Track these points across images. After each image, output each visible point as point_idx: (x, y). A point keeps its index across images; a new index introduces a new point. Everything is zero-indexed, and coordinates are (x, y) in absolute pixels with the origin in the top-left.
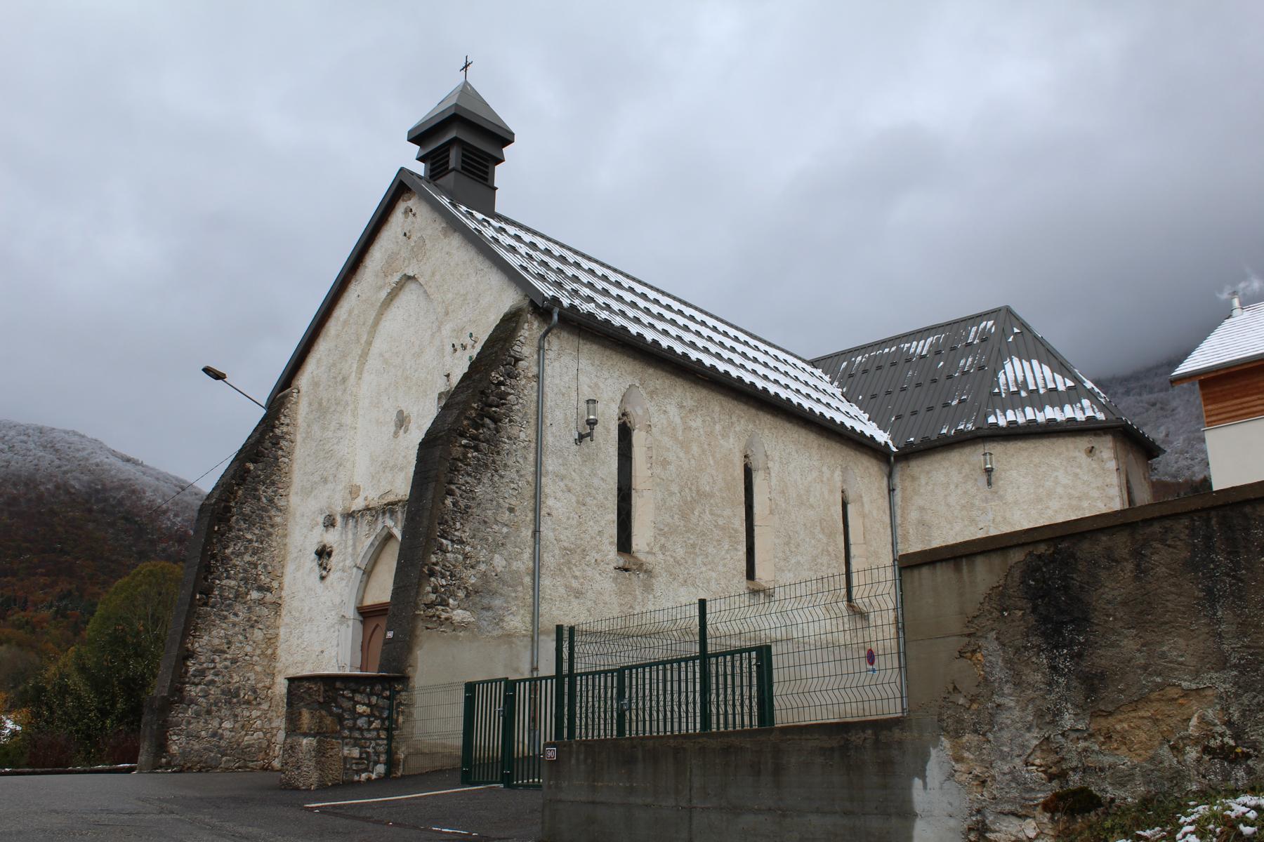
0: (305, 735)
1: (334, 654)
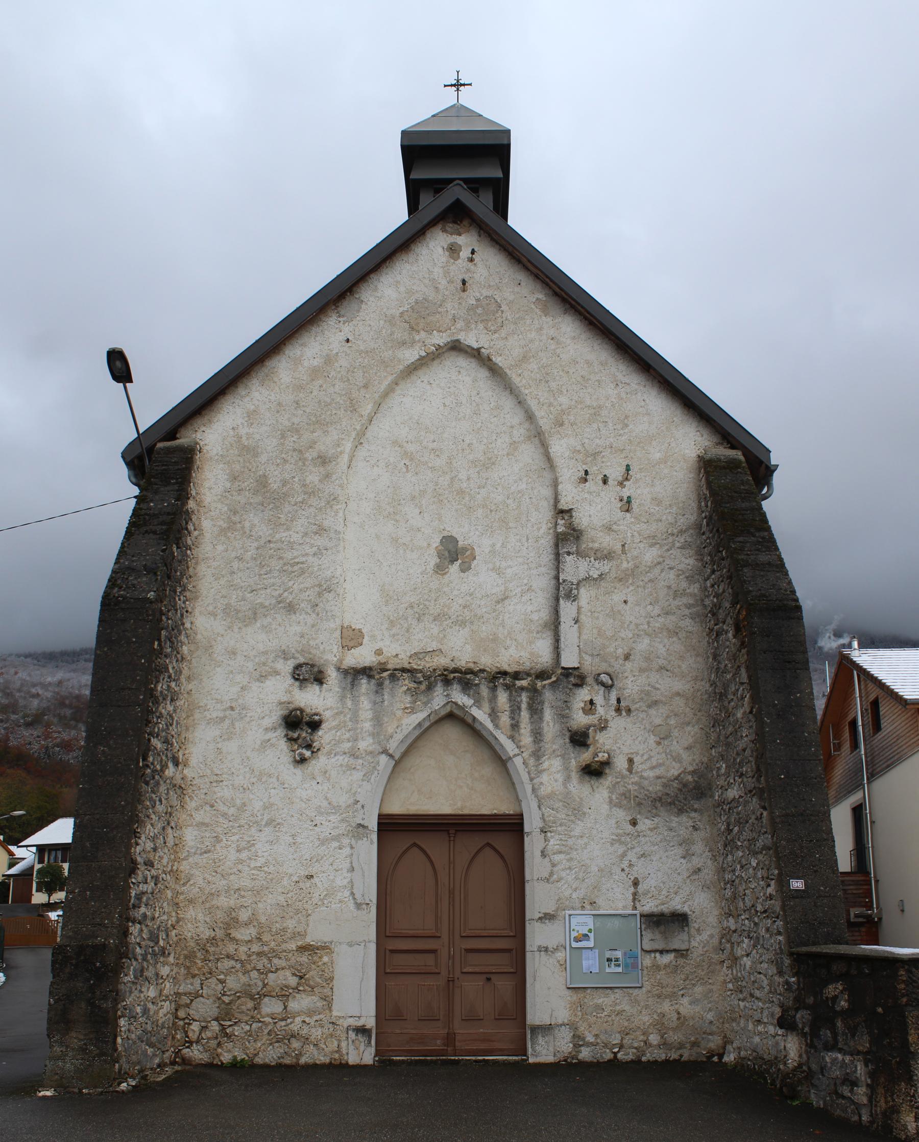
1: (341, 880)
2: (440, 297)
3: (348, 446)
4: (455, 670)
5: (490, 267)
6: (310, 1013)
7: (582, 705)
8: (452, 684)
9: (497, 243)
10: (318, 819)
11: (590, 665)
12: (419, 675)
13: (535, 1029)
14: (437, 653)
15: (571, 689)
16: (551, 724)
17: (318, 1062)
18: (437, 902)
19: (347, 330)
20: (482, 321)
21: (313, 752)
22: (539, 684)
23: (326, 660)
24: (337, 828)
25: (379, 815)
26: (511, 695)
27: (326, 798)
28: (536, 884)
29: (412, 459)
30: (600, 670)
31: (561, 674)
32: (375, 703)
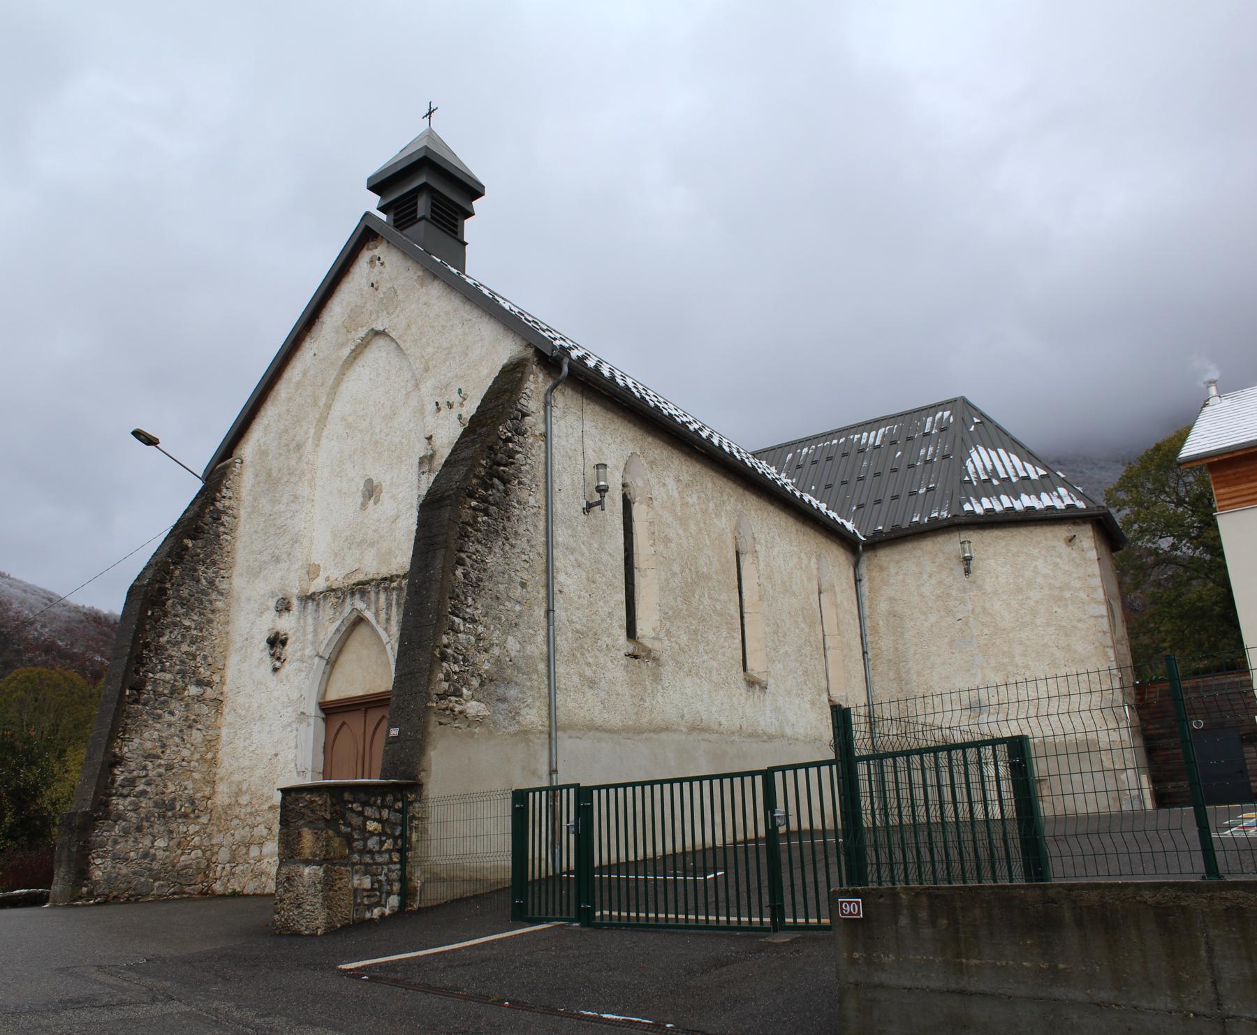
0: (307, 862)
1: (291, 757)
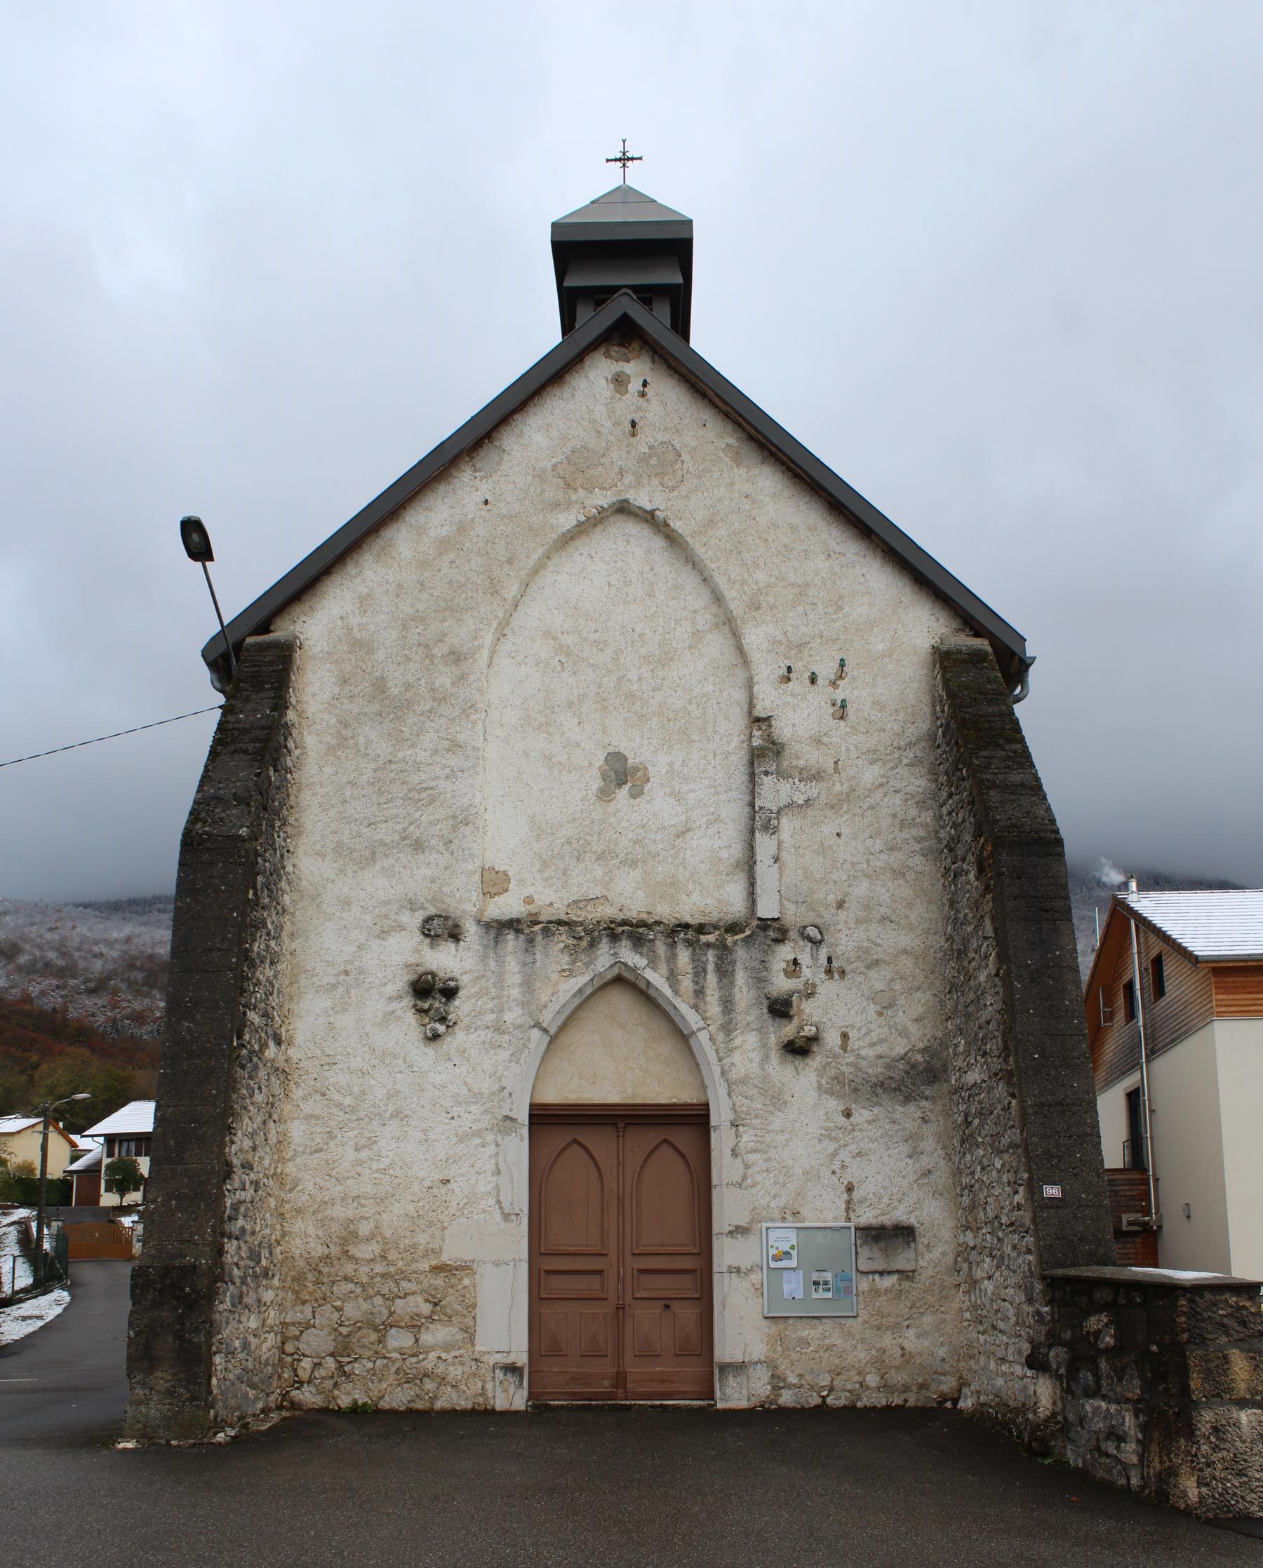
2: (603, 444)
3: (488, 639)
4: (624, 923)
5: (667, 403)
6: (447, 1347)
7: (784, 965)
8: (620, 940)
9: (676, 371)
10: (455, 1111)
11: (793, 916)
12: (580, 929)
13: (724, 1368)
14: (602, 901)
15: (769, 946)
16: (745, 990)
17: (458, 1408)
18: (602, 1211)
19: (484, 489)
20: (657, 475)
21: (448, 1027)
22: (729, 939)
23: (464, 911)
24: (479, 1120)
25: (531, 1105)
26: (694, 953)
27: (465, 1084)
28: (725, 1189)
29: (568, 655)
30: (807, 921)
31: (757, 926)
32: (524, 964)
